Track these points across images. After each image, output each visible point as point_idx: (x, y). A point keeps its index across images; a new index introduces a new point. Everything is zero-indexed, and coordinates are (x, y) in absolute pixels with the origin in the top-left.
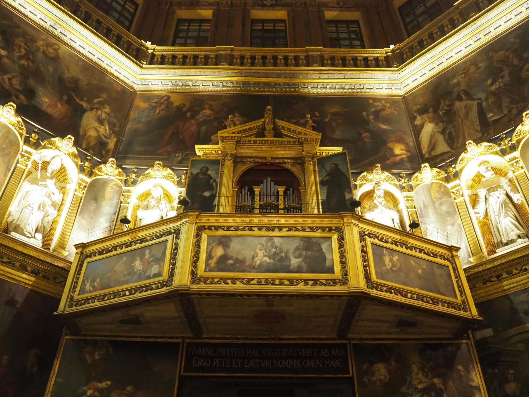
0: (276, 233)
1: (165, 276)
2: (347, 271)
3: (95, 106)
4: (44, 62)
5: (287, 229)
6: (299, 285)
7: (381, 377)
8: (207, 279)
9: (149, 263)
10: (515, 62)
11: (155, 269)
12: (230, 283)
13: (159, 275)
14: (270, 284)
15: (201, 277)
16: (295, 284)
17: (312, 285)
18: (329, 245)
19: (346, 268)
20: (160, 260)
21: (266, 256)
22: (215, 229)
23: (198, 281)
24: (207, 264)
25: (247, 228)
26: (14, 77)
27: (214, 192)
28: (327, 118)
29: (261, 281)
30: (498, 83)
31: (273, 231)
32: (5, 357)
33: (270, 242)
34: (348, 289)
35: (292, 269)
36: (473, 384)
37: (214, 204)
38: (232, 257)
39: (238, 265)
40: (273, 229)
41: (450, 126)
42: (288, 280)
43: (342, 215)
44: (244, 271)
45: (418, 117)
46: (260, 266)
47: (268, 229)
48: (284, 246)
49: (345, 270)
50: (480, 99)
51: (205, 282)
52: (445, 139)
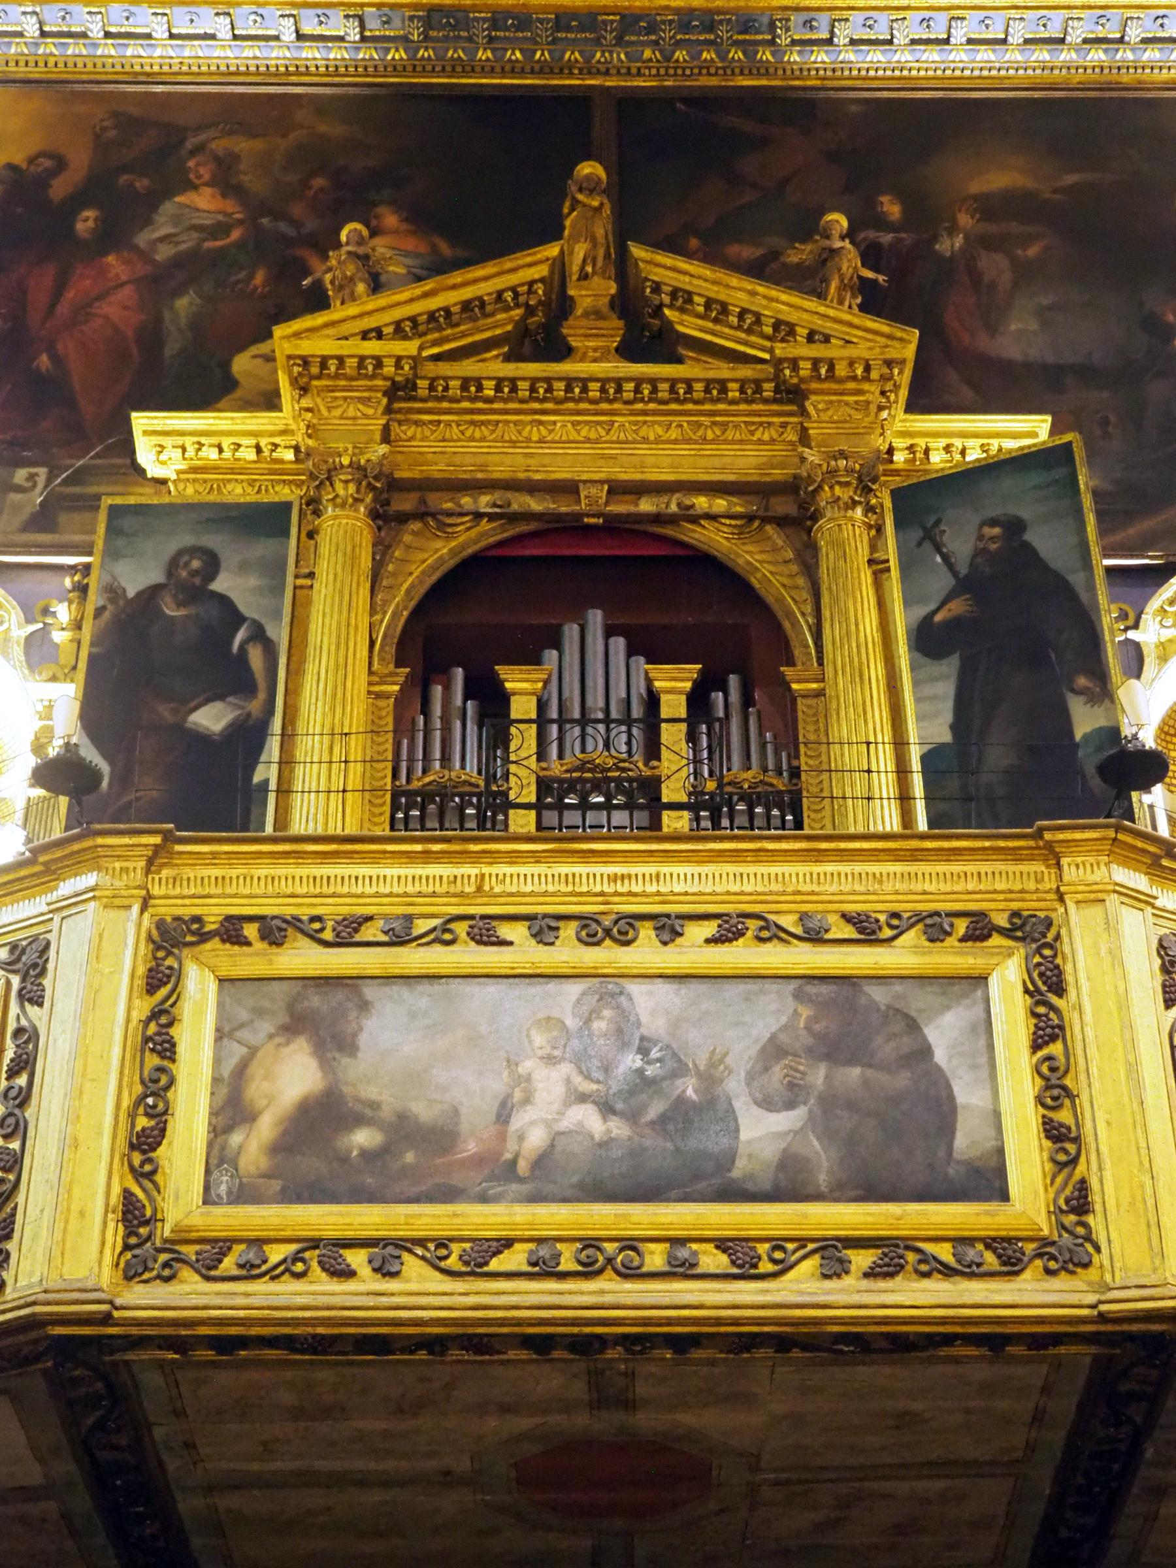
2: (1083, 1187)
5: (710, 929)
6: (791, 1275)
8: (223, 1246)
12: (365, 1271)
14: (609, 1272)
15: (183, 1237)
16: (766, 1267)
17: (870, 1274)
18: (974, 1029)
19: (1081, 1169)
21: (583, 1098)
22: (265, 935)
23: (166, 1265)
25: (461, 928)
27: (255, 706)
29: (557, 1256)
31: (627, 943)
33: (607, 1013)
34: (1092, 1299)
35: (750, 1177)
37: (257, 778)
38: (375, 1105)
39: (410, 1157)
42: (722, 1244)
43: (1048, 836)
44: (448, 1194)
46: (542, 1161)
48: (693, 1036)
49: (1077, 1175)
51: (208, 1269)
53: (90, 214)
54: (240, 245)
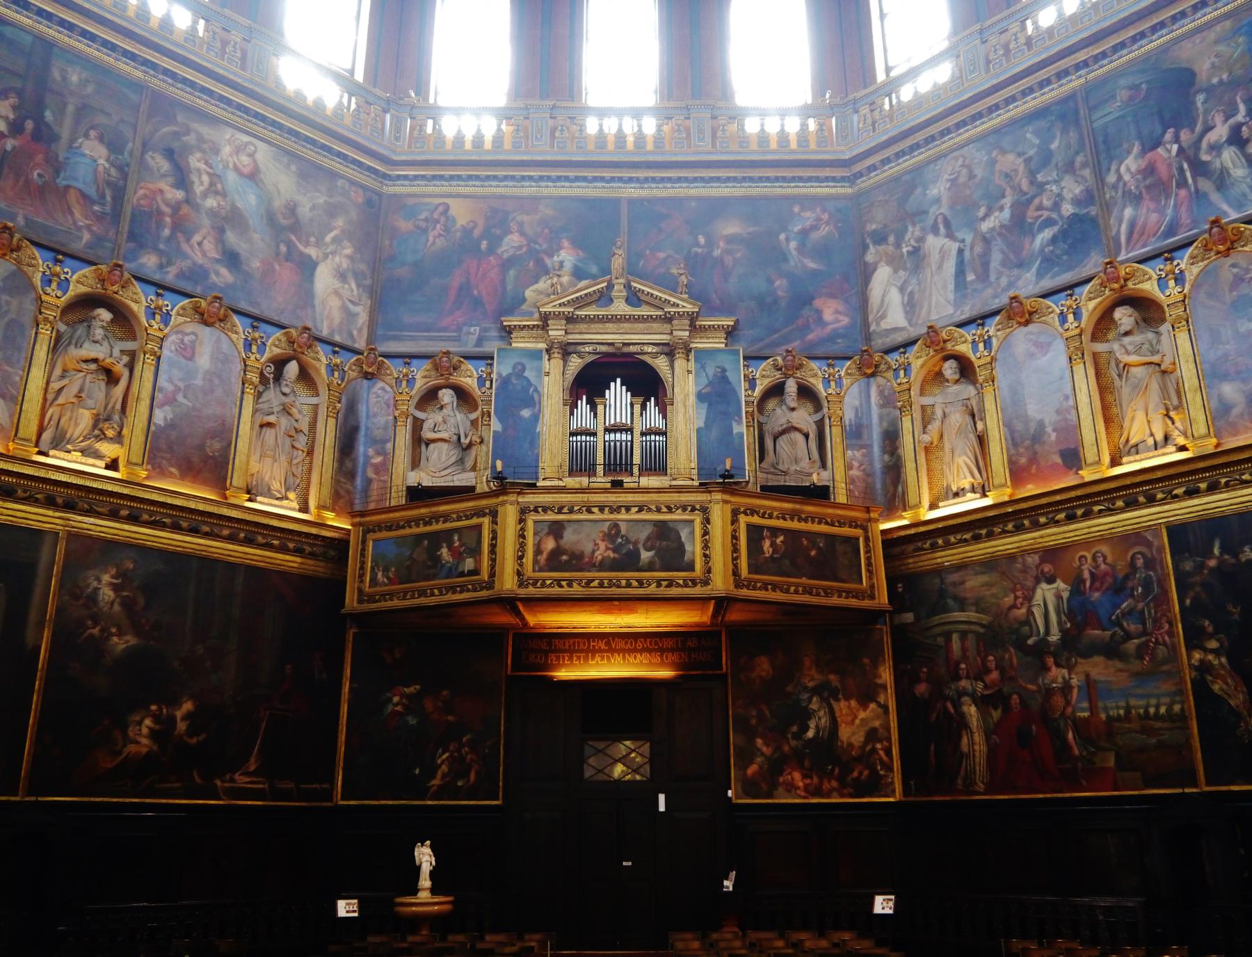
0: (623, 516)
1: (485, 575)
2: (710, 568)
3: (328, 251)
4: (240, 189)
5: (636, 509)
7: (763, 674)
8: (537, 581)
9: (460, 554)
10: (1025, 185)
11: (469, 564)
13: (475, 572)
15: (529, 578)
17: (666, 587)
20: (476, 552)
24: (535, 562)
25: (584, 509)
26: (204, 238)
28: (718, 247)
30: (992, 218)
32: (288, 667)
36: (879, 681)
40: (617, 510)
41: (914, 281)
42: (637, 581)
45: (871, 246)
46: (601, 562)
47: (612, 511)
50: (963, 241)
51: (534, 585)
52: (903, 302)
53: (485, 242)
54: (525, 253)
